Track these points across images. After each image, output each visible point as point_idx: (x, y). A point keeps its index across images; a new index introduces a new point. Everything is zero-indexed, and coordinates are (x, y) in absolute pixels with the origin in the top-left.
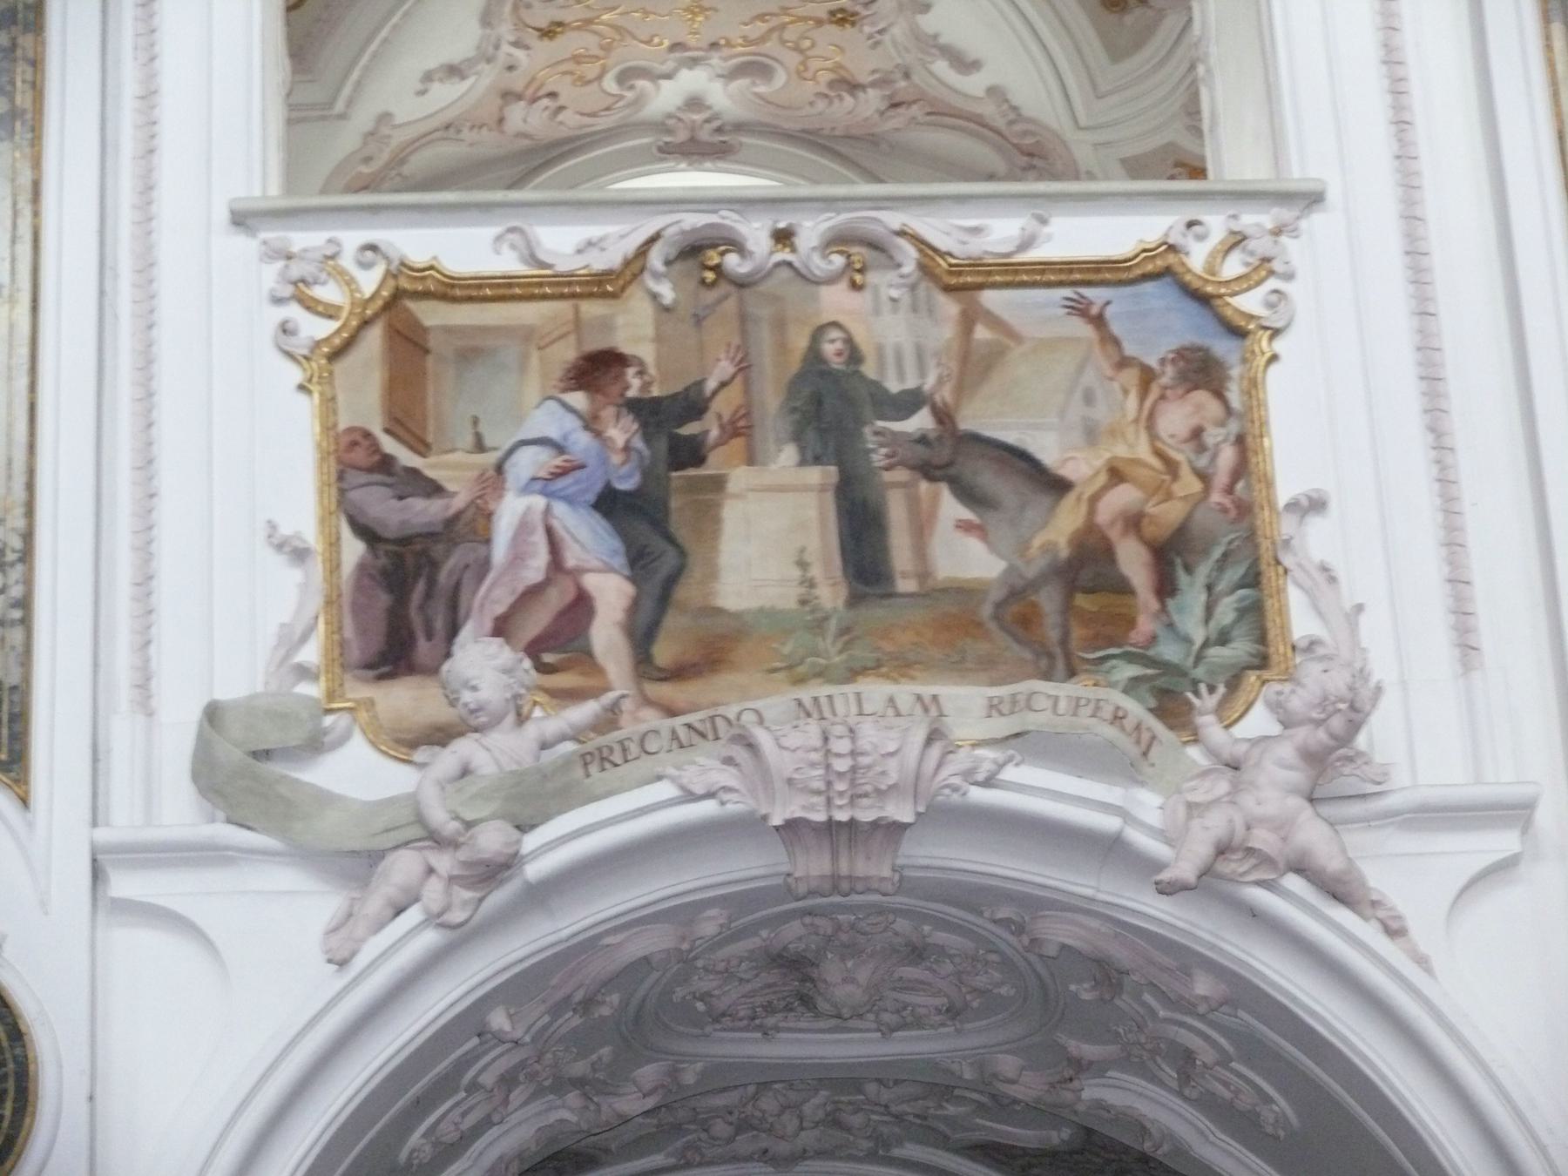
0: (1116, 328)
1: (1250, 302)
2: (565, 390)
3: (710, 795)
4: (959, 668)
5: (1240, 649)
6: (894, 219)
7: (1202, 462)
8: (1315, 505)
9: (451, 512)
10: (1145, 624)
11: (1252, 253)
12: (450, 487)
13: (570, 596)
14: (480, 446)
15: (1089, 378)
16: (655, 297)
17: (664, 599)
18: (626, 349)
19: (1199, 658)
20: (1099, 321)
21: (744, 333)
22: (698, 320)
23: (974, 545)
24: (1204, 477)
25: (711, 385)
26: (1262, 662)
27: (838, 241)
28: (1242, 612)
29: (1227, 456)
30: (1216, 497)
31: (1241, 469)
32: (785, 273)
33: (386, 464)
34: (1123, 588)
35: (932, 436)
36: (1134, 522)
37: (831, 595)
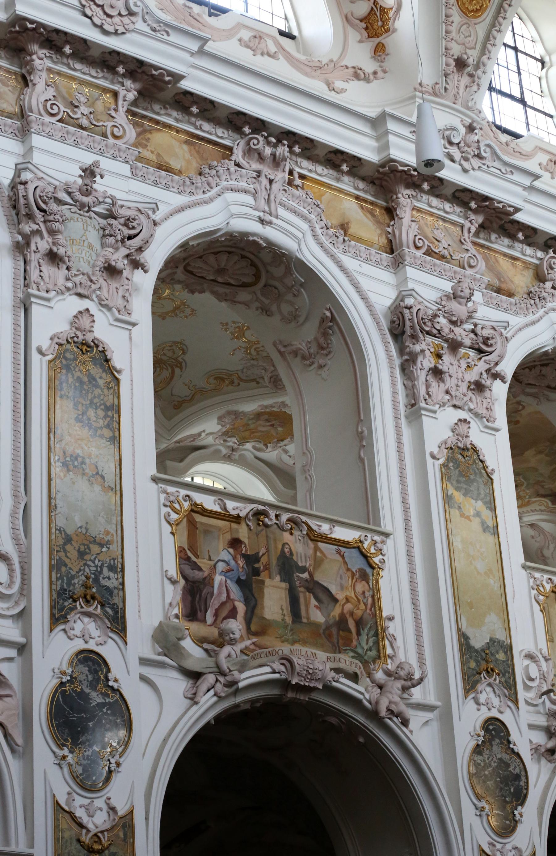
0: (347, 560)
1: (376, 560)
2: (228, 548)
3: (279, 673)
4: (322, 647)
5: (373, 653)
6: (304, 518)
7: (365, 601)
8: (391, 619)
9: (204, 576)
10: (355, 642)
11: (378, 547)
12: (204, 569)
13: (232, 606)
14: (210, 559)
15: (341, 572)
16: (248, 525)
17: (253, 612)
18: (242, 539)
19: (366, 654)
20: (343, 557)
21: (268, 541)
22: (257, 535)
23: (318, 612)
24: (365, 605)
25: (261, 554)
26: (379, 658)
27: (289, 520)
28: (374, 643)
29: (370, 600)
30: (368, 611)
31: (373, 604)
32: (275, 526)
33: (188, 559)
34: (350, 631)
35: (309, 580)
36: (352, 614)
37: (289, 620)
